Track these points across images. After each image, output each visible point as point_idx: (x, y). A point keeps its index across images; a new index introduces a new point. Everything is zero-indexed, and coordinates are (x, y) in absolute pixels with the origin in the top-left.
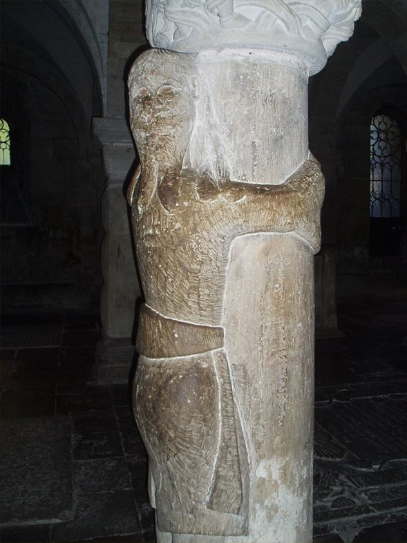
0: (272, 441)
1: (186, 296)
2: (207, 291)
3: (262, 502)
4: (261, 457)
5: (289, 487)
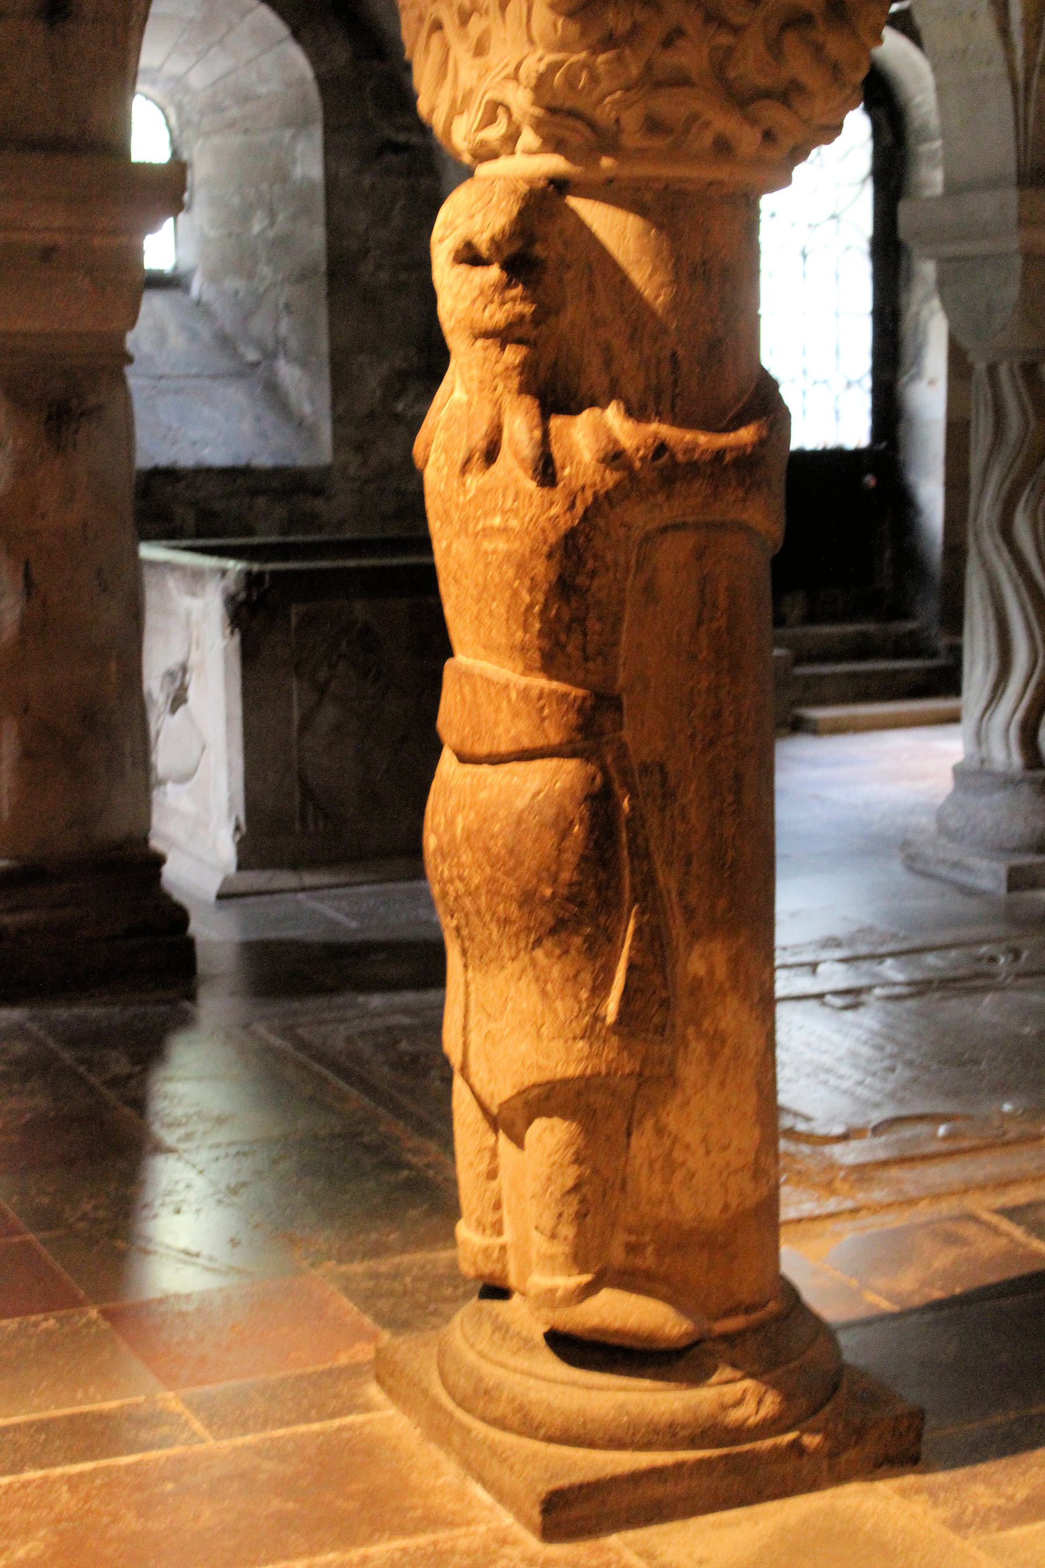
0: (713, 907)
1: (563, 637)
2: (598, 627)
3: (698, 1024)
4: (695, 936)
5: (744, 998)
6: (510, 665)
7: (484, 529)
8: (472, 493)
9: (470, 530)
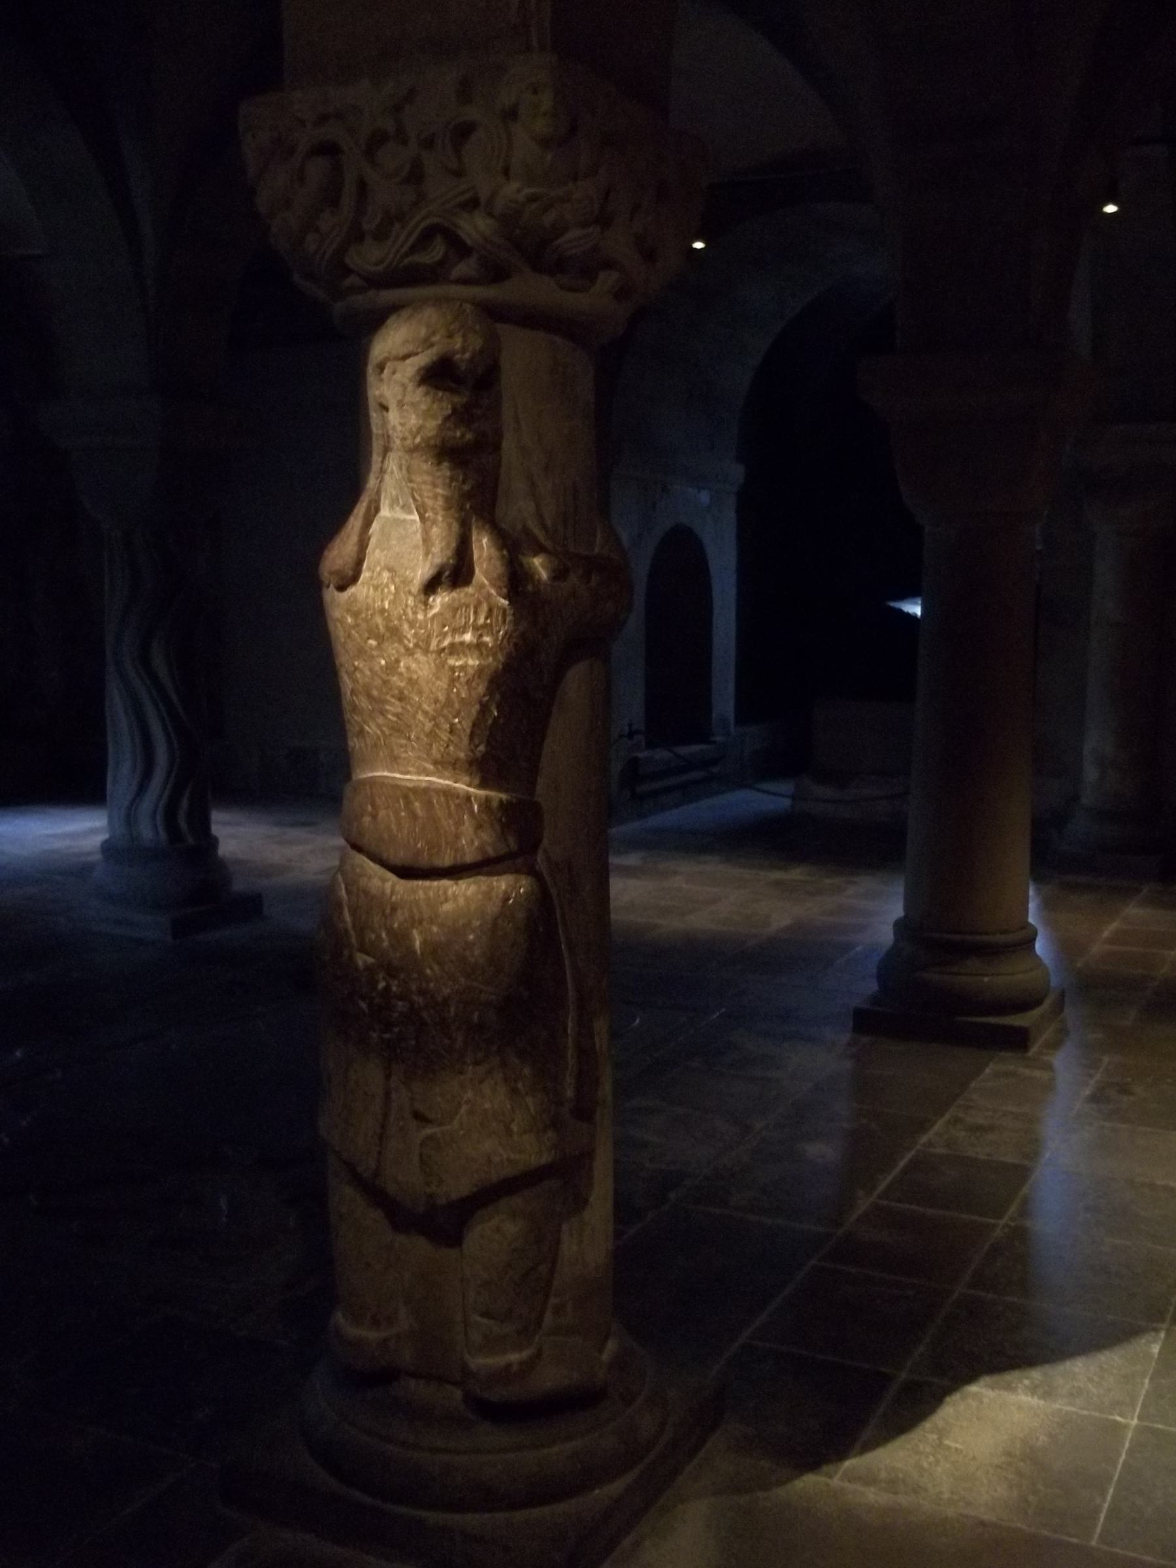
6: (467, 779)
7: (452, 645)
8: (436, 610)
9: (433, 645)
